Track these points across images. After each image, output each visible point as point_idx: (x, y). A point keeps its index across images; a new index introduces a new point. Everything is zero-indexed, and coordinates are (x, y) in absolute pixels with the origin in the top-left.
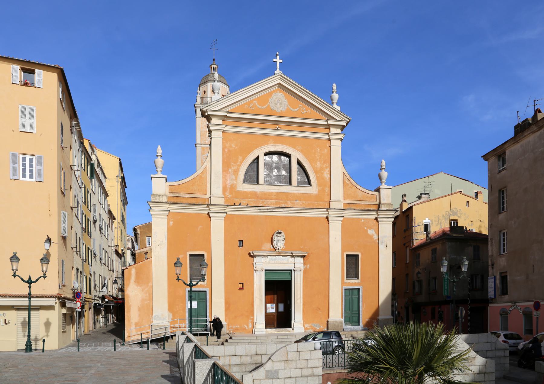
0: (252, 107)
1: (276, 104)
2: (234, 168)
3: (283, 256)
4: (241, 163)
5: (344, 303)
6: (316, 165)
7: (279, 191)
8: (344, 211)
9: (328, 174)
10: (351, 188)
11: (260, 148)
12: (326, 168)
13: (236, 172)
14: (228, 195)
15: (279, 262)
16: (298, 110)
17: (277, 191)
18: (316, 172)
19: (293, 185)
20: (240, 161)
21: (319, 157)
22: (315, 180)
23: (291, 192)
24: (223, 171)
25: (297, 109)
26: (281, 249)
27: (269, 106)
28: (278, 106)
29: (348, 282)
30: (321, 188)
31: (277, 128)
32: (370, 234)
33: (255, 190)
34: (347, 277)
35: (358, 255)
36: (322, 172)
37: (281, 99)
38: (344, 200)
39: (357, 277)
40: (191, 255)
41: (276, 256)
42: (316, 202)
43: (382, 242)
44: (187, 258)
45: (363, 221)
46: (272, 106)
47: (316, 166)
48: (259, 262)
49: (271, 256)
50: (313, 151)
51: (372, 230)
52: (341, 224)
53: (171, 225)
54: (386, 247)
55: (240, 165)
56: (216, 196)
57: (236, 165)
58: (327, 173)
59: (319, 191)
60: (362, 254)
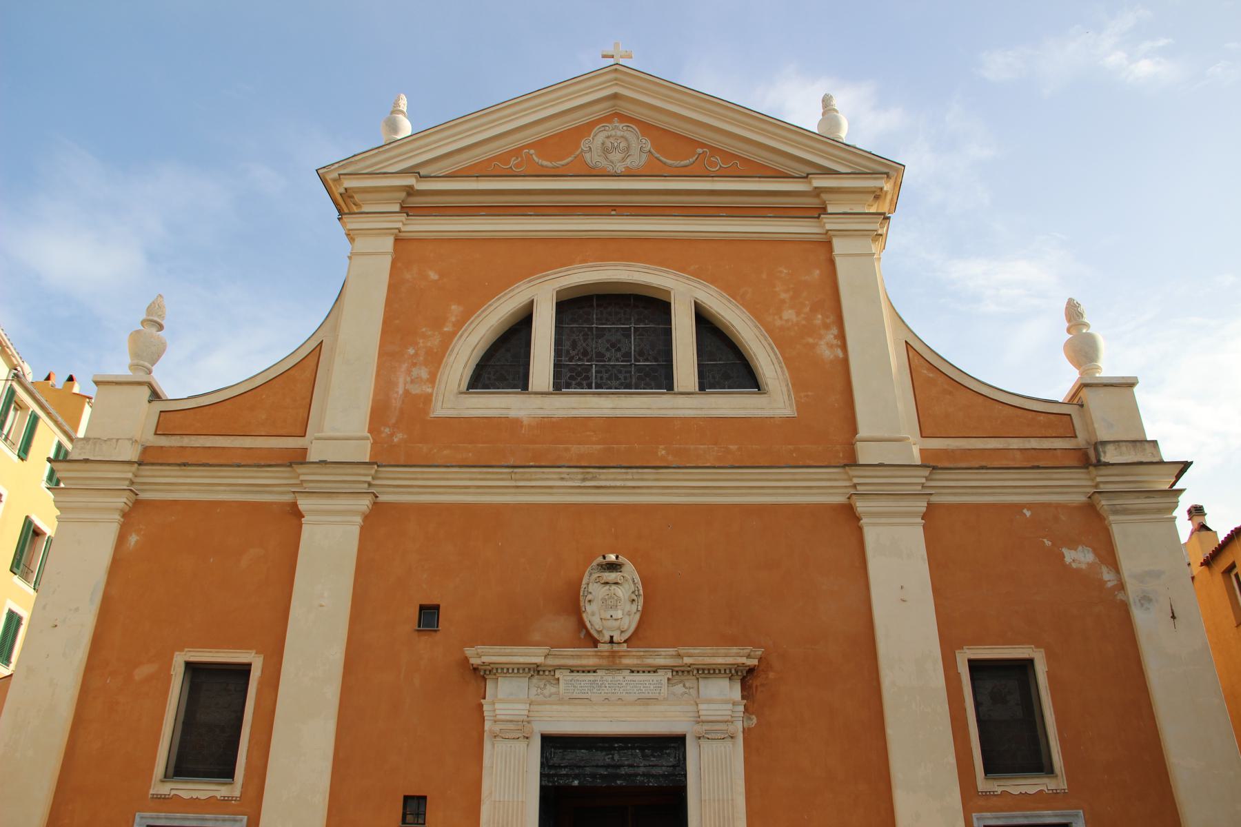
2: (429, 344)
4: (460, 324)
6: (781, 318)
7: (618, 413)
8: (926, 472)
12: (827, 327)
13: (436, 359)
14: (392, 435)
18: (781, 340)
19: (681, 390)
20: (453, 319)
21: (791, 293)
22: (779, 370)
23: (671, 413)
24: (381, 354)
25: (688, 161)
26: (625, 642)
28: (616, 156)
29: (999, 790)
32: (1074, 565)
33: (513, 414)
34: (990, 769)
36: (811, 340)
37: (626, 140)
38: (922, 437)
40: (188, 665)
41: (600, 673)
42: (791, 447)
43: (1146, 599)
45: (1028, 514)
46: (594, 158)
47: (778, 323)
50: (764, 276)
51: (1080, 548)
53: (131, 548)
55: (455, 333)
57: (437, 333)
58: (831, 346)
60: (1050, 657)
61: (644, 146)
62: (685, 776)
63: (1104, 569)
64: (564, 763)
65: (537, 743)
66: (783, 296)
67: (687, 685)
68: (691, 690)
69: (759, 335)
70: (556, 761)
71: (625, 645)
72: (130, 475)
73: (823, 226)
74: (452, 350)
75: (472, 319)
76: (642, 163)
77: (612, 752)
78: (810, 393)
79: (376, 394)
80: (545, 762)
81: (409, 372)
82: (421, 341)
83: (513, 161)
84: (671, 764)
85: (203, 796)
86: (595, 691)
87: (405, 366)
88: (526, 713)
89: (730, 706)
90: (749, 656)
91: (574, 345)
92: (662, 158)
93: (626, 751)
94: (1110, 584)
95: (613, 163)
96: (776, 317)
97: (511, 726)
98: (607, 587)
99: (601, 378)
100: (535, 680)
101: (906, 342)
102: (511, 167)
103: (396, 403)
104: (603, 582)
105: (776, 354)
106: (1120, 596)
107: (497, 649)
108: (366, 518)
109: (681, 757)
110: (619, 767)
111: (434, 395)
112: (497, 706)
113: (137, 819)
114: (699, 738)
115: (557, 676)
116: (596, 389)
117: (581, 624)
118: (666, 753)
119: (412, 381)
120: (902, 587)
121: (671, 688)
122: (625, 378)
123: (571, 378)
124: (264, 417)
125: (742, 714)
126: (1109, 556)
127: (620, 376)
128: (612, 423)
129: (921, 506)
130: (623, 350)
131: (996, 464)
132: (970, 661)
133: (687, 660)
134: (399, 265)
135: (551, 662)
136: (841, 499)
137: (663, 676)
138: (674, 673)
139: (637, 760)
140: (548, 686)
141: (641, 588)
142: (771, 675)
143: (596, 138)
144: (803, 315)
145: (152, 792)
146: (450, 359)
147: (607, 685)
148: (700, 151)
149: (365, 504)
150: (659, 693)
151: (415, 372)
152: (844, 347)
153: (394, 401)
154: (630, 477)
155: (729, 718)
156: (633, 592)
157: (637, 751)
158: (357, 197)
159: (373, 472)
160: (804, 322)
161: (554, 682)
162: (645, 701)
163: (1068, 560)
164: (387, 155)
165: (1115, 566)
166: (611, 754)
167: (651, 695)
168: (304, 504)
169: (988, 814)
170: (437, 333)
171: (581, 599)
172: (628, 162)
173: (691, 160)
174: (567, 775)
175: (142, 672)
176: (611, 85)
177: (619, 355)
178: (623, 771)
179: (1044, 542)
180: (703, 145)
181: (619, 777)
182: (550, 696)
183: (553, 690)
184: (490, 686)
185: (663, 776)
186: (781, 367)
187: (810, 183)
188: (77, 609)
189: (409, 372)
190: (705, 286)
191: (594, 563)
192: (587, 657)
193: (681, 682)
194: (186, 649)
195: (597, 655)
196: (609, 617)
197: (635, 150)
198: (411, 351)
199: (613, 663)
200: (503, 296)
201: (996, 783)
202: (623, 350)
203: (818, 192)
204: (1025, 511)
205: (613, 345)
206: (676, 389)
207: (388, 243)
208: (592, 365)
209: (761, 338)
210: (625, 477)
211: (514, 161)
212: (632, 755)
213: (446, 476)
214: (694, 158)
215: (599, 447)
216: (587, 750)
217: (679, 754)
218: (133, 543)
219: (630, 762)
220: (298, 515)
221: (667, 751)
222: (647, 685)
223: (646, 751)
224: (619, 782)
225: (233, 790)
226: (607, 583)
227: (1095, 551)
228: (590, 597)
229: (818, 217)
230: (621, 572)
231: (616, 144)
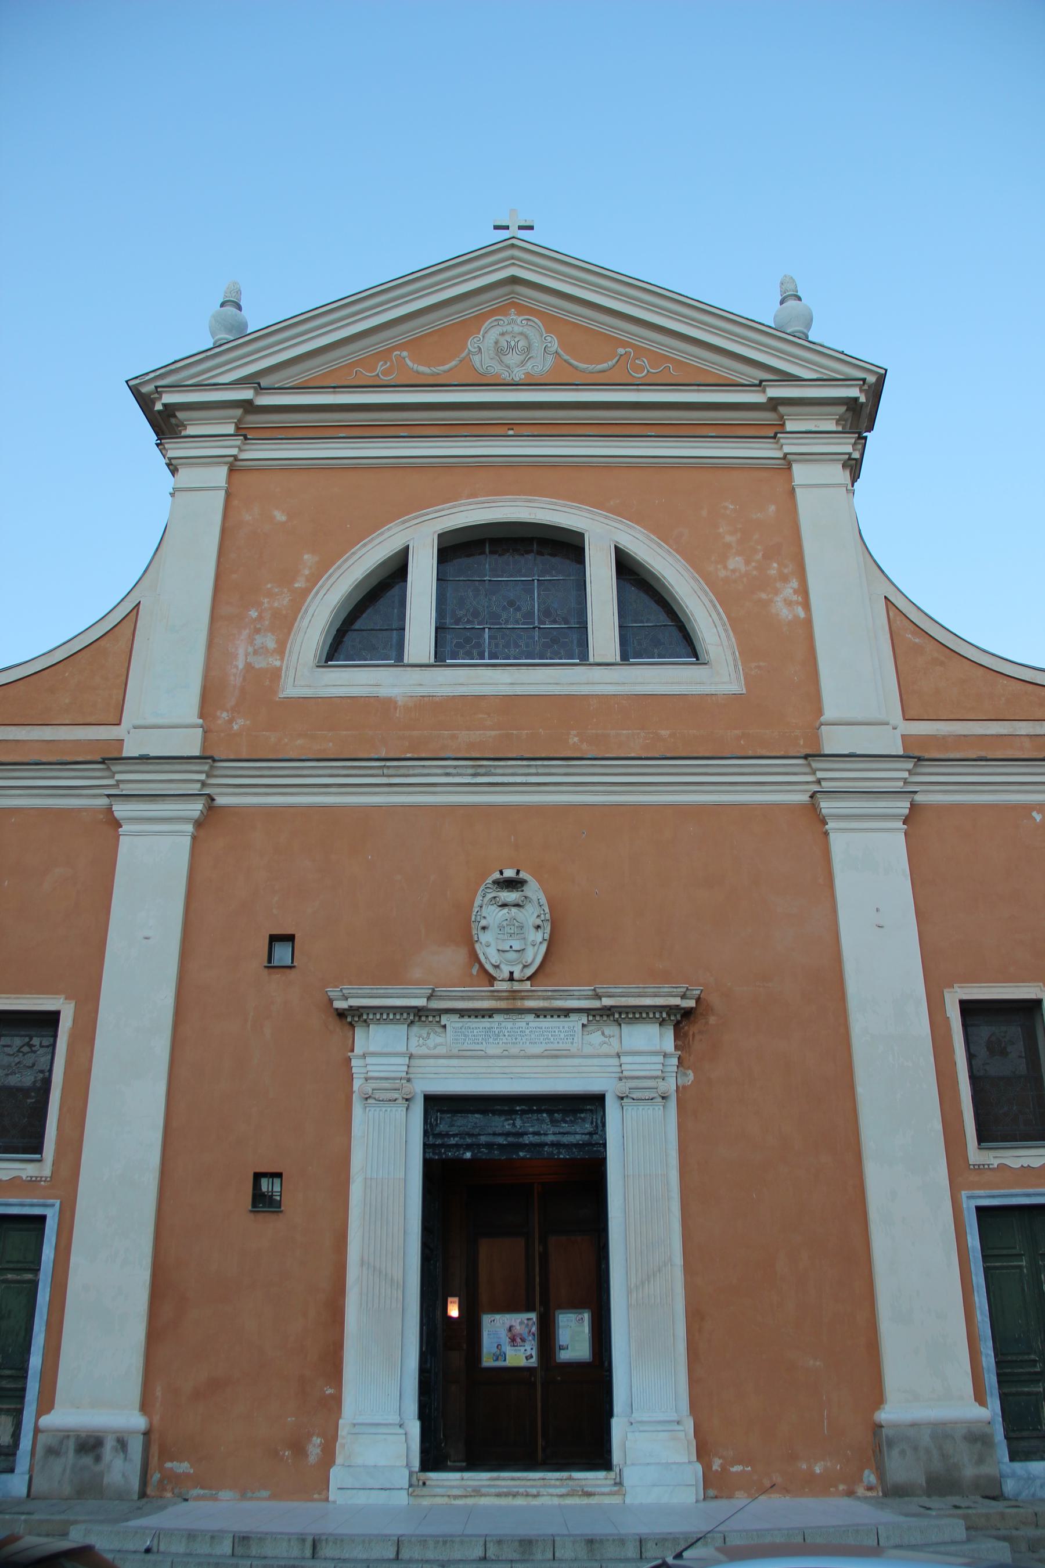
2: (276, 604)
3: (538, 1013)
4: (314, 579)
5: (981, 1300)
6: (725, 567)
7: (519, 690)
10: (942, 664)
12: (785, 579)
14: (231, 721)
15: (514, 1050)
19: (598, 660)
20: (307, 572)
21: (739, 535)
22: (723, 635)
23: (585, 690)
26: (528, 979)
27: (467, 362)
28: (512, 359)
29: (995, 1163)
30: (759, 667)
33: (383, 692)
34: (983, 1137)
36: (764, 596)
37: (526, 337)
41: (497, 1018)
42: (738, 732)
45: (1038, 817)
46: (485, 362)
47: (722, 573)
48: (385, 1050)
49: (462, 1013)
56: (160, 721)
58: (789, 603)
61: (549, 345)
62: (604, 1145)
64: (454, 1130)
65: (418, 1109)
66: (729, 539)
68: (611, 1039)
69: (696, 588)
70: (442, 1128)
71: (529, 983)
74: (306, 611)
76: (547, 367)
77: (513, 1117)
78: (762, 664)
80: (429, 1130)
81: (251, 641)
83: (380, 367)
84: (586, 1131)
86: (491, 1040)
87: (245, 633)
88: (405, 1068)
89: (660, 1059)
90: (683, 997)
93: (530, 1115)
95: (509, 367)
96: (719, 566)
98: (505, 910)
99: (497, 645)
100: (415, 1029)
101: (885, 597)
102: (378, 375)
104: (500, 904)
105: (719, 614)
107: (367, 989)
108: (199, 824)
109: (599, 1122)
110: (522, 1134)
111: (284, 668)
114: (622, 1098)
115: (443, 1023)
116: (489, 659)
117: (474, 957)
118: (581, 1118)
119: (255, 652)
120: (877, 910)
122: (527, 646)
123: (459, 645)
124: (67, 701)
125: (675, 1069)
127: (522, 643)
128: (510, 703)
129: (903, 807)
130: (524, 609)
131: (958, 756)
132: (962, 1003)
133: (607, 1002)
134: (235, 502)
137: (576, 1022)
138: (591, 1018)
139: (544, 1126)
140: (432, 1035)
141: (547, 910)
142: (712, 1020)
144: (753, 564)
147: (507, 1034)
148: (621, 351)
149: (196, 808)
150: (572, 1043)
151: (259, 640)
152: (806, 605)
153: (232, 678)
155: (659, 1073)
156: (538, 916)
157: (545, 1115)
158: (180, 415)
159: (206, 768)
160: (755, 573)
161: (439, 1030)
166: (511, 1120)
168: (121, 810)
169: (981, 1192)
170: (285, 590)
172: (529, 366)
174: (457, 1146)
177: (519, 615)
178: (526, 1140)
180: (624, 344)
182: (435, 1048)
183: (439, 1040)
184: (359, 1033)
185: (577, 1145)
186: (726, 631)
187: (764, 392)
190: (630, 527)
191: (490, 880)
195: (495, 996)
196: (508, 948)
198: (254, 614)
200: (370, 541)
201: (992, 1154)
202: (524, 609)
204: (1034, 814)
205: (512, 604)
206: (591, 660)
209: (700, 593)
210: (527, 771)
211: (382, 366)
212: (538, 1119)
214: (615, 361)
215: (493, 733)
216: (481, 1114)
217: (597, 1119)
219: (536, 1129)
220: (117, 824)
221: (582, 1115)
222: (557, 1033)
223: (556, 1115)
224: (521, 1154)
226: (504, 905)
228: (483, 923)
229: (774, 437)
230: (522, 891)
231: (513, 344)
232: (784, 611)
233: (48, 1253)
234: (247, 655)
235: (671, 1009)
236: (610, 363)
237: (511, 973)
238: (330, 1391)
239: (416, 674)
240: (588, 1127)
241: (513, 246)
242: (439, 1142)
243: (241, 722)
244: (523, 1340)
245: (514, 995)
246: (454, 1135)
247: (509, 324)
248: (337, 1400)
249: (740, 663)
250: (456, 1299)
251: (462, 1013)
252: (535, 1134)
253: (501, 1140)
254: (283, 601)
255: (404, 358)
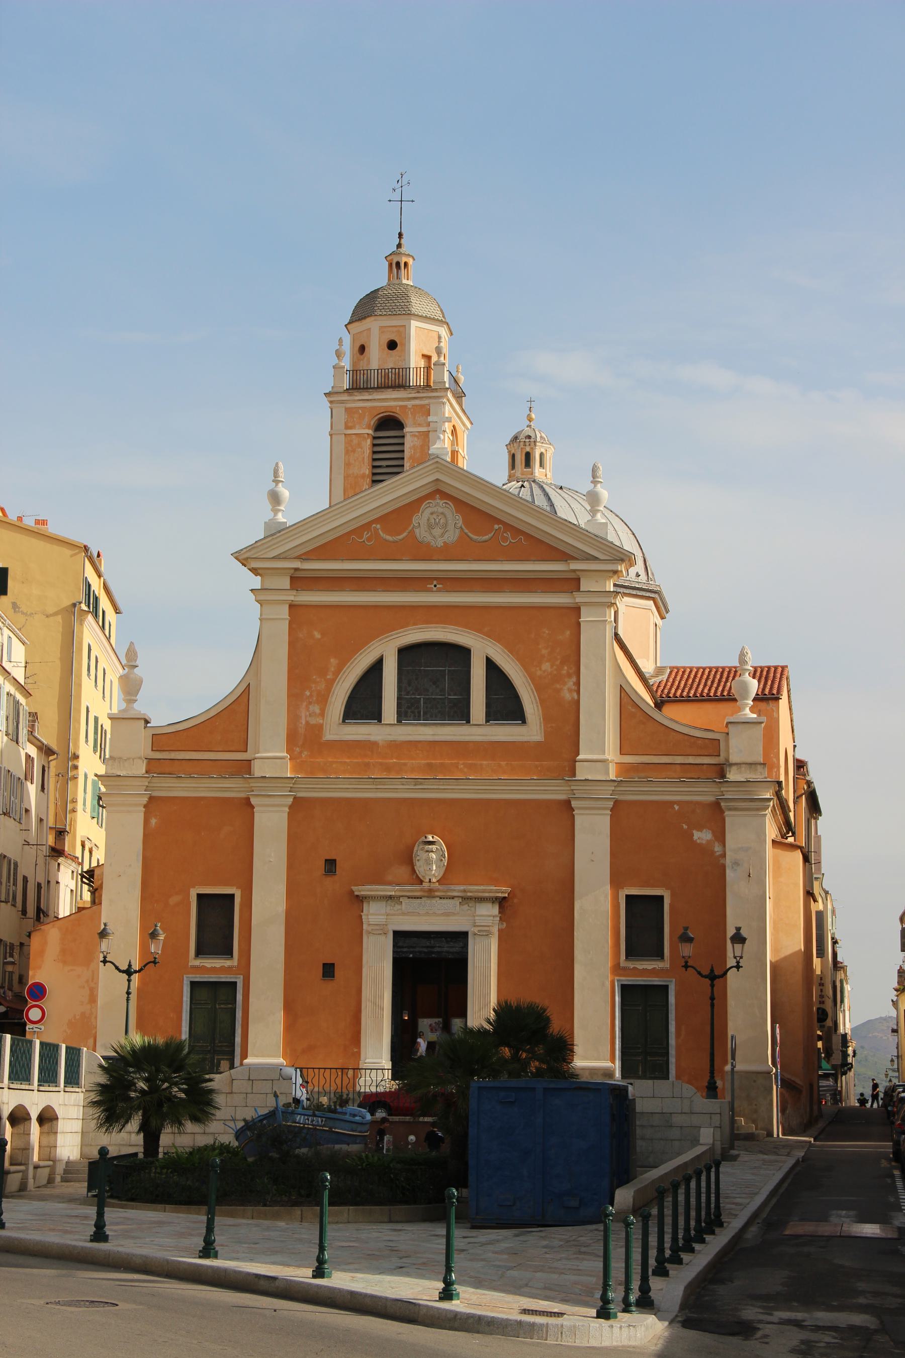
0: (369, 539)
1: (430, 527)
4: (337, 673)
7: (437, 738)
9: (575, 690)
11: (386, 637)
12: (569, 676)
13: (323, 699)
16: (492, 537)
17: (431, 738)
18: (540, 687)
20: (333, 669)
22: (536, 709)
23: (467, 738)
26: (438, 881)
28: (437, 531)
29: (632, 966)
31: (433, 586)
32: (698, 841)
33: (372, 738)
35: (660, 898)
36: (558, 686)
38: (620, 754)
39: (660, 955)
40: (200, 896)
41: (424, 899)
44: (189, 904)
45: (676, 807)
46: (422, 534)
47: (539, 673)
49: (409, 897)
51: (705, 830)
52: (608, 819)
53: (153, 826)
54: (747, 876)
58: (570, 690)
59: (547, 734)
60: (673, 895)
62: (467, 953)
63: (717, 844)
65: (391, 936)
67: (470, 905)
69: (525, 682)
70: (400, 944)
72: (147, 784)
73: (575, 598)
74: (334, 693)
75: (345, 669)
76: (455, 539)
78: (554, 725)
79: (288, 725)
81: (307, 708)
82: (313, 686)
83: (365, 536)
85: (218, 966)
87: (305, 704)
91: (409, 684)
92: (470, 534)
94: (717, 854)
95: (434, 538)
96: (537, 668)
97: (377, 927)
99: (427, 707)
102: (364, 541)
103: (302, 730)
105: (535, 697)
106: (722, 861)
108: (290, 807)
110: (433, 947)
111: (324, 724)
112: (370, 917)
113: (185, 978)
117: (414, 871)
119: (310, 715)
120: (592, 853)
121: (462, 907)
123: (409, 707)
126: (720, 836)
132: (627, 896)
133: (469, 894)
135: (398, 894)
136: (563, 797)
137: (457, 902)
142: (516, 901)
143: (423, 515)
144: (555, 667)
145: (190, 964)
146: (332, 699)
148: (496, 527)
151: (311, 708)
154: (441, 783)
156: (442, 856)
160: (555, 672)
162: (447, 914)
163: (695, 838)
164: (279, 539)
165: (723, 843)
167: (450, 911)
168: (253, 801)
170: (323, 680)
171: (414, 858)
172: (446, 536)
173: (490, 535)
175: (174, 900)
176: (432, 473)
178: (436, 950)
179: (683, 826)
180: (499, 521)
181: (433, 953)
182: (397, 911)
186: (537, 706)
188: (130, 866)
189: (307, 708)
190: (492, 643)
192: (415, 890)
193: (464, 904)
194: (197, 887)
195: (421, 890)
197: (451, 527)
198: (308, 693)
199: (430, 894)
200: (364, 652)
203: (574, 571)
206: (471, 723)
207: (286, 608)
208: (420, 698)
209: (527, 684)
210: (439, 783)
211: (366, 534)
213: (335, 783)
214: (492, 534)
218: (154, 824)
220: (253, 807)
224: (433, 955)
225: (234, 962)
226: (427, 851)
227: (714, 833)
228: (418, 858)
229: (572, 592)
231: (437, 520)
232: (567, 696)
233: (239, 997)
234: (306, 716)
235: (497, 898)
236: (490, 535)
237: (430, 879)
238: (356, 1050)
239: (388, 730)
240: (461, 944)
241: (437, 460)
242: (399, 950)
243: (306, 753)
244: (436, 1030)
245: (431, 890)
246: (405, 947)
247: (435, 506)
248: (359, 1053)
249: (542, 725)
250: (407, 1012)
251: (409, 897)
252: (439, 947)
253: (425, 950)
254: (322, 686)
255: (378, 529)
